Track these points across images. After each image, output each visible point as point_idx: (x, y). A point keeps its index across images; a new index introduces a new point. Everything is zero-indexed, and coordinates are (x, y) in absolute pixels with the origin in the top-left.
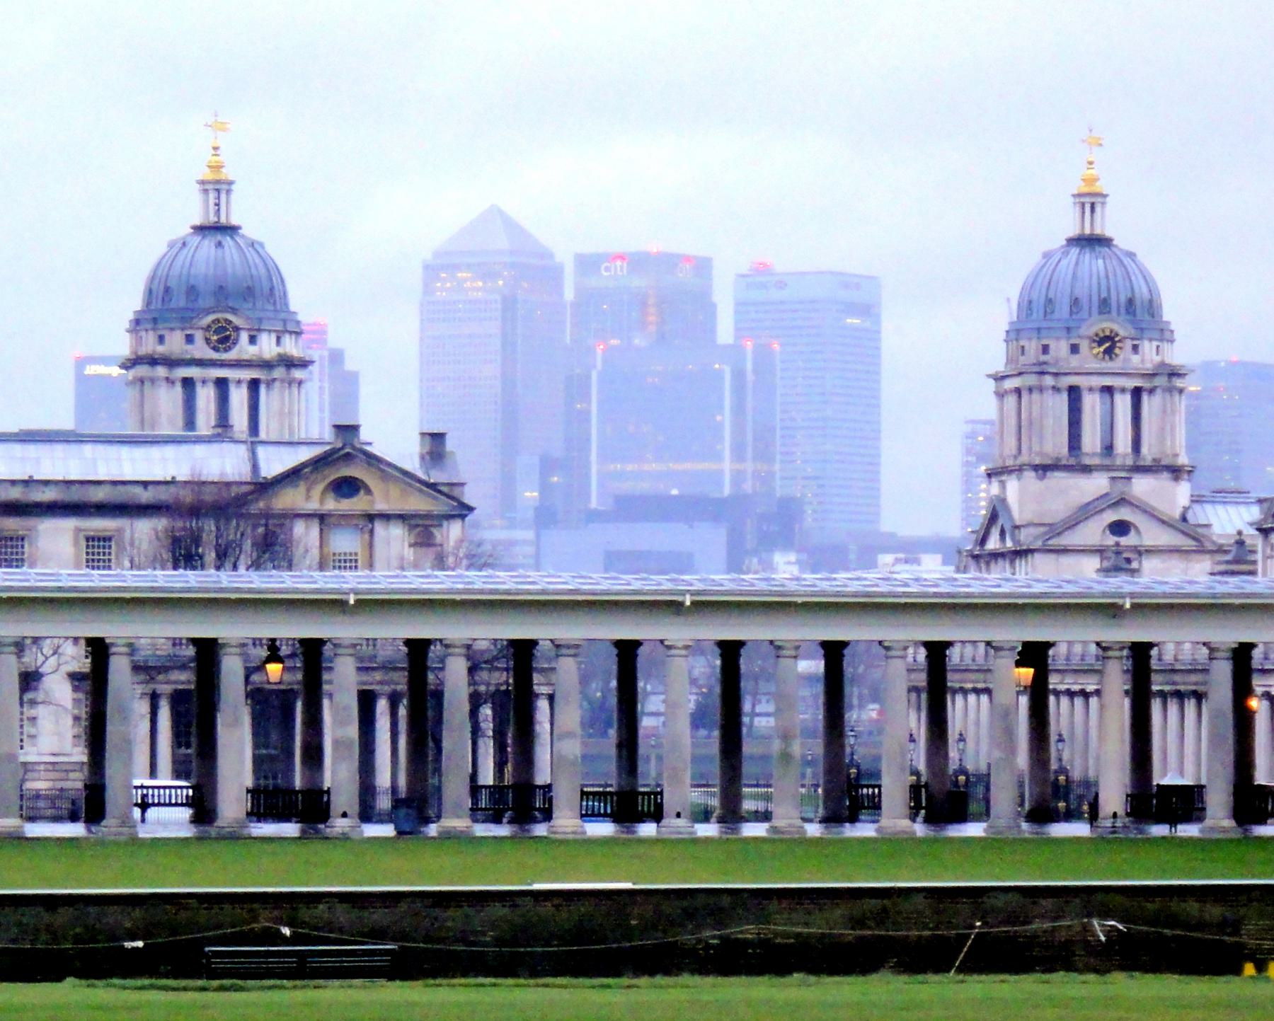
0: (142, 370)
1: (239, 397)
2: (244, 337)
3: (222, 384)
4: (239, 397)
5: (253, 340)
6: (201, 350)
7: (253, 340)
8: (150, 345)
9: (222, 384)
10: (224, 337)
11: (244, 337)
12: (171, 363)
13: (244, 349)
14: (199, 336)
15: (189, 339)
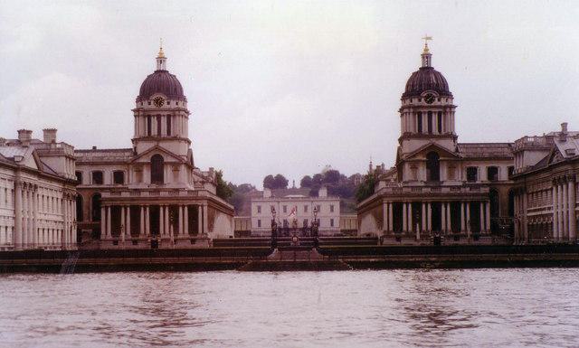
0: (406, 110)
1: (435, 118)
2: (436, 99)
3: (430, 114)
4: (435, 118)
5: (439, 100)
6: (423, 102)
7: (439, 100)
8: (408, 102)
9: (430, 114)
10: (430, 99)
11: (436, 99)
12: (414, 107)
13: (436, 103)
14: (423, 99)
15: (420, 100)
